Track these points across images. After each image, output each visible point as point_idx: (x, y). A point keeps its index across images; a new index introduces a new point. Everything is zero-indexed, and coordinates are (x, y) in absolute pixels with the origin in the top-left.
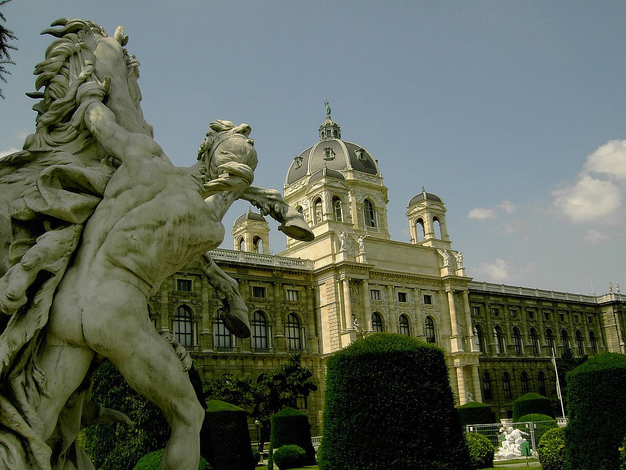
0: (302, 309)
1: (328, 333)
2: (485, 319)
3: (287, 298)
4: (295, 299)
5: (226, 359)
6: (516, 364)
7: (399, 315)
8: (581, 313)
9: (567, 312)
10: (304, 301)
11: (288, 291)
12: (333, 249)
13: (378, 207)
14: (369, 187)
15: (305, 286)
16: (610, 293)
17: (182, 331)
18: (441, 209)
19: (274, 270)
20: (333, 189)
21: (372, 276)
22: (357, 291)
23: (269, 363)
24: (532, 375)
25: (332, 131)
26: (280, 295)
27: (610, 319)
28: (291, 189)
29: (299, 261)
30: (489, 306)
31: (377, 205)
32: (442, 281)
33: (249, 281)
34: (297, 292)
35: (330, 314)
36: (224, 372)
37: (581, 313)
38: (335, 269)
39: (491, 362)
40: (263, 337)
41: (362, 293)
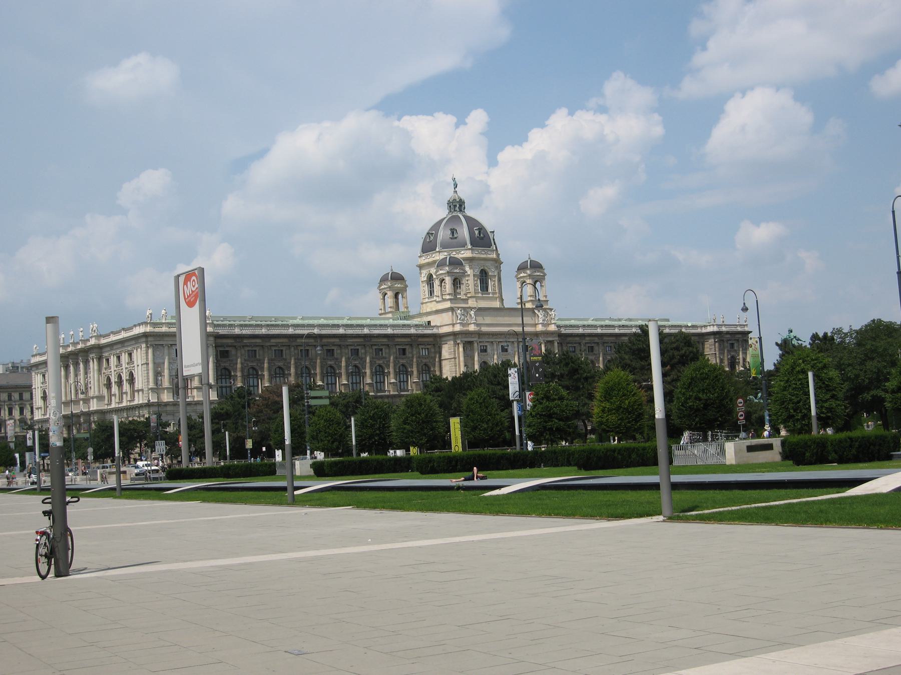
0: (431, 361)
3: (421, 354)
4: (427, 354)
10: (433, 355)
12: (453, 320)
14: (485, 259)
15: (434, 345)
17: (354, 381)
20: (452, 274)
25: (458, 206)
28: (424, 258)
33: (395, 345)
34: (428, 349)
35: (450, 365)
38: (454, 334)
41: (472, 350)
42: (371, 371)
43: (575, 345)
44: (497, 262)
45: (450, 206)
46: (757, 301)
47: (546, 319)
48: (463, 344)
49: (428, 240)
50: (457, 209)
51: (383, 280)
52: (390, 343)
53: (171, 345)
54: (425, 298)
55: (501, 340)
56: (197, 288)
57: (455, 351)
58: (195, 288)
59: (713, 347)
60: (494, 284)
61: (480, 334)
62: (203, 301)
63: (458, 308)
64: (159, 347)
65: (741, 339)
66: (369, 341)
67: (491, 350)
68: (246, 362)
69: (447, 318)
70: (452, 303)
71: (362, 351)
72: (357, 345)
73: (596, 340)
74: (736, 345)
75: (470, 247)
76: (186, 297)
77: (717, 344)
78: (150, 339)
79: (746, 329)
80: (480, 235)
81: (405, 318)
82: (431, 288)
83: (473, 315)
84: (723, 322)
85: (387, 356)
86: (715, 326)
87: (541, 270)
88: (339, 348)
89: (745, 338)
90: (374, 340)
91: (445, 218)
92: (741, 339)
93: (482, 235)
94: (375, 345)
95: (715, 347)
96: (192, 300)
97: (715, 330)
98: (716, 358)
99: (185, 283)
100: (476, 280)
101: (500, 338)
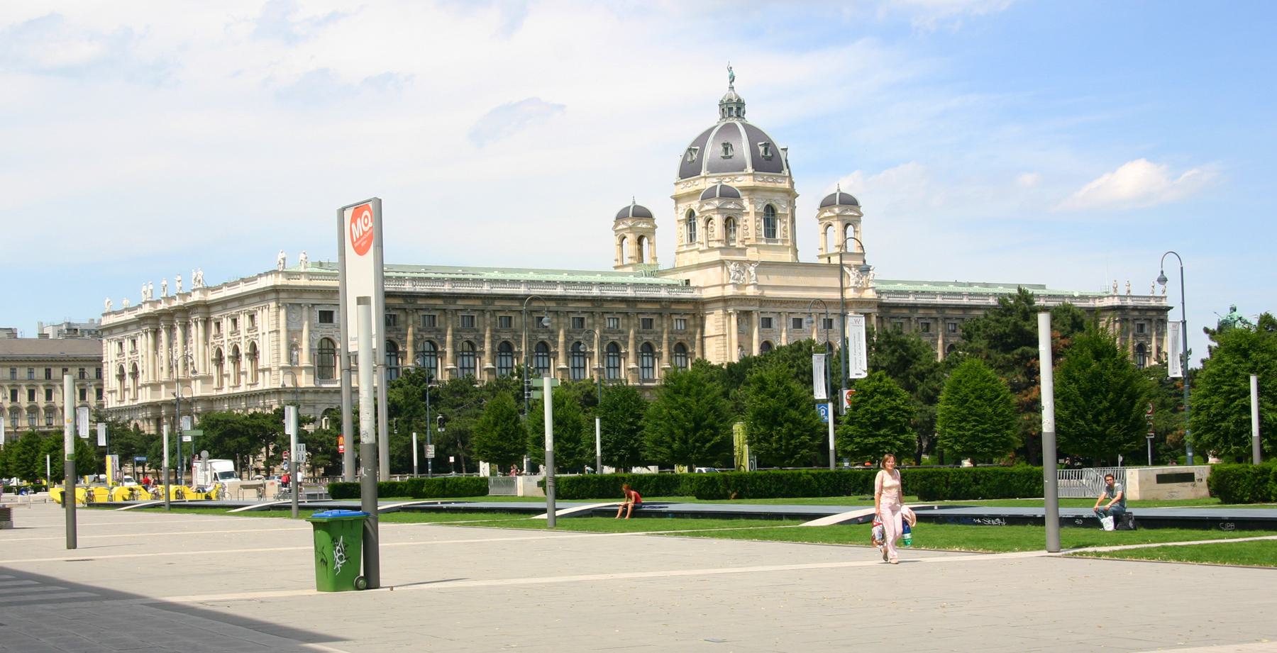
0: (689, 338)
3: (675, 328)
4: (683, 328)
10: (692, 330)
11: (677, 320)
12: (722, 279)
14: (772, 190)
15: (694, 314)
18: (856, 214)
20: (725, 211)
25: (735, 109)
28: (682, 186)
33: (638, 313)
34: (685, 320)
35: (717, 345)
38: (725, 301)
41: (750, 324)
44: (791, 195)
45: (723, 110)
46: (1182, 268)
47: (861, 282)
48: (737, 314)
49: (689, 160)
51: (622, 216)
52: (630, 310)
53: (313, 305)
54: (683, 246)
55: (792, 310)
56: (370, 228)
57: (724, 325)
58: (368, 228)
60: (785, 227)
61: (762, 301)
62: (380, 245)
63: (732, 261)
64: (295, 306)
65: (1156, 319)
66: (599, 307)
67: (778, 325)
68: (421, 333)
69: (714, 275)
70: (722, 254)
71: (588, 321)
72: (582, 312)
73: (934, 313)
75: (750, 170)
76: (355, 240)
78: (282, 295)
79: (1164, 303)
80: (766, 153)
81: (652, 274)
82: (691, 231)
83: (753, 273)
84: (1129, 291)
85: (625, 329)
86: (1116, 298)
87: (855, 207)
88: (556, 316)
89: (1161, 317)
90: (607, 305)
91: (715, 127)
93: (769, 154)
94: (607, 313)
96: (362, 245)
97: (1116, 304)
99: (354, 220)
100: (758, 221)
101: (791, 307)
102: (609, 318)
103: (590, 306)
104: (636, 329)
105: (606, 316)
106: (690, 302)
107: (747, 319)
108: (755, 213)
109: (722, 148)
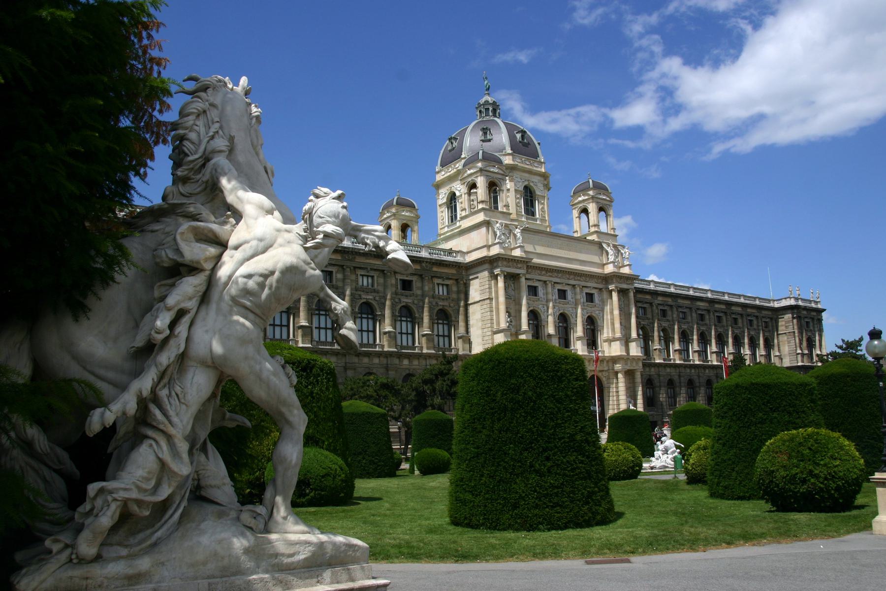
0: (452, 305)
1: (480, 332)
2: (651, 321)
4: (445, 293)
5: (369, 357)
6: (682, 370)
7: (558, 314)
8: (757, 317)
9: (742, 315)
10: (454, 296)
12: (487, 240)
13: (539, 195)
14: (530, 172)
15: (457, 280)
16: (788, 296)
19: (423, 261)
20: (489, 174)
21: (529, 270)
22: (513, 285)
23: (416, 362)
24: (699, 383)
25: (491, 109)
26: (429, 288)
27: (787, 325)
28: (443, 173)
29: (450, 252)
30: (657, 307)
31: (538, 193)
32: (606, 278)
34: (447, 285)
35: (483, 311)
36: (367, 371)
37: (757, 317)
38: (490, 262)
39: (656, 368)
40: (409, 334)
41: (518, 289)
42: (353, 310)
43: (645, 306)
48: (505, 276)
49: (450, 148)
50: (491, 114)
57: (490, 288)
59: (791, 324)
60: (543, 208)
66: (349, 260)
67: (544, 295)
69: (479, 237)
70: (486, 215)
73: (669, 301)
74: (811, 324)
75: (510, 151)
77: (795, 321)
79: (820, 306)
82: (452, 213)
83: (519, 235)
85: (381, 289)
86: (792, 299)
89: (819, 317)
92: (816, 318)
95: (793, 325)
98: (795, 337)
100: (518, 198)
102: (363, 276)
103: (340, 258)
104: (394, 289)
105: (359, 272)
106: (453, 265)
107: (514, 283)
108: (515, 190)
109: (481, 133)
